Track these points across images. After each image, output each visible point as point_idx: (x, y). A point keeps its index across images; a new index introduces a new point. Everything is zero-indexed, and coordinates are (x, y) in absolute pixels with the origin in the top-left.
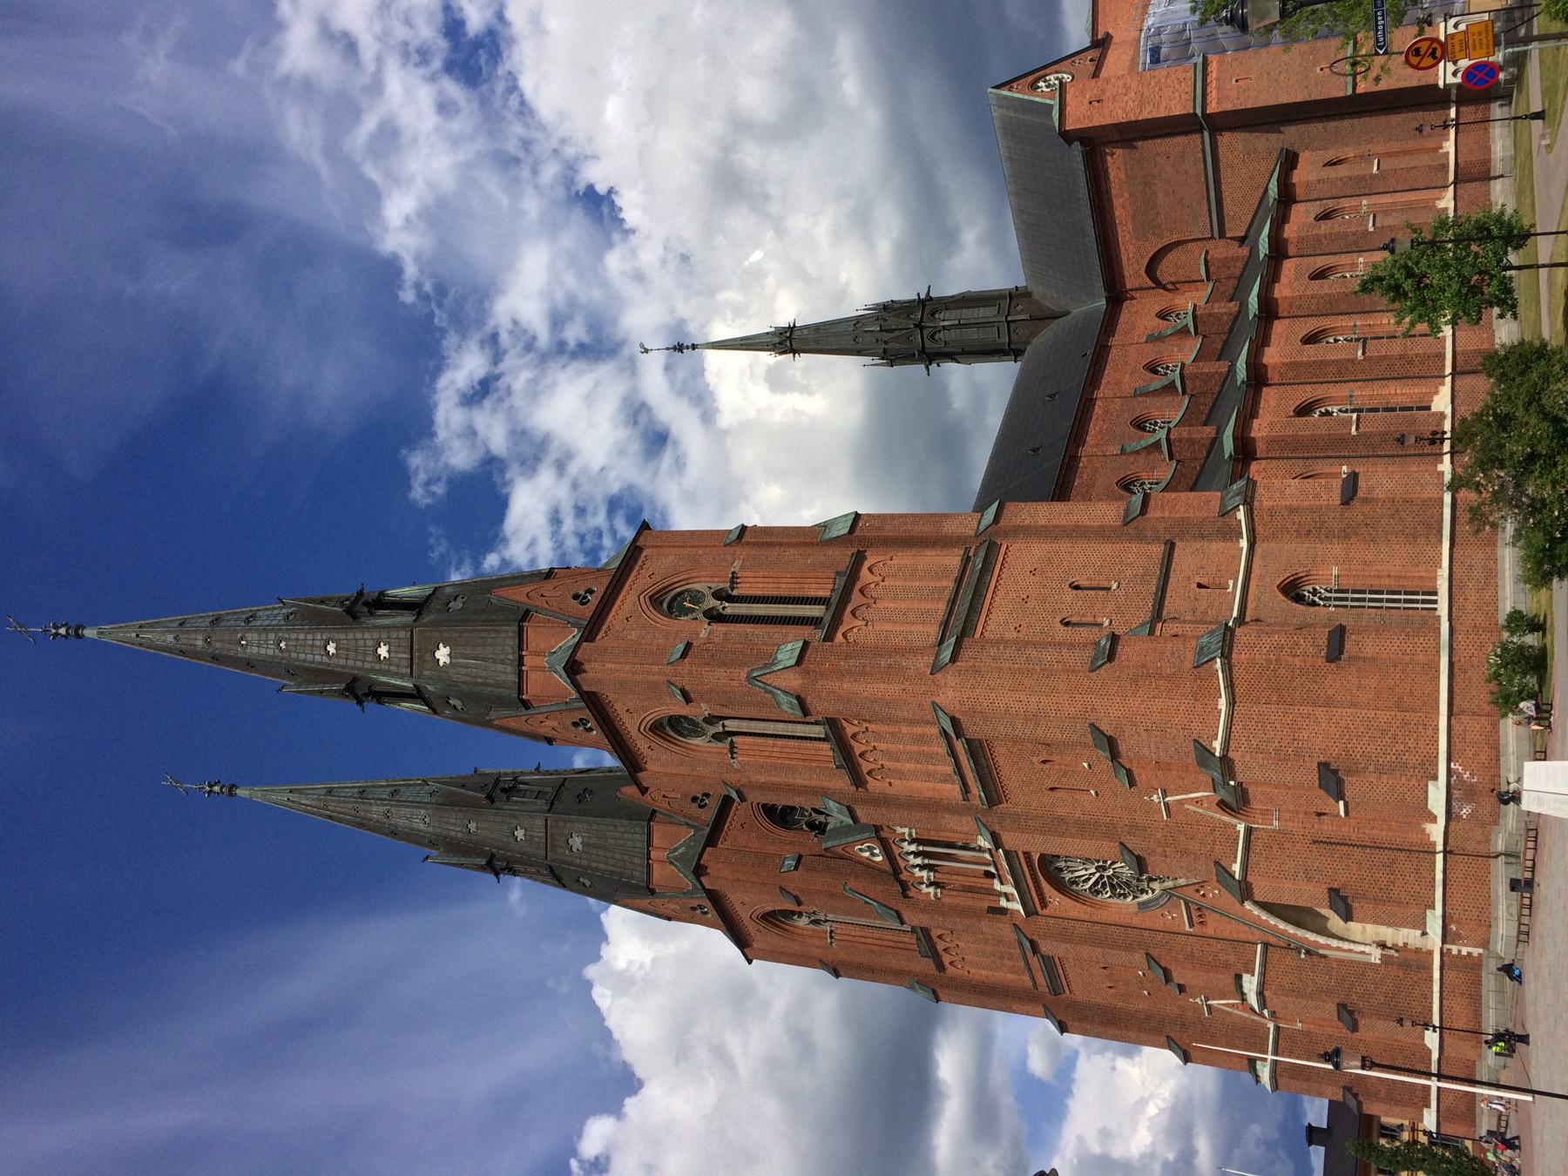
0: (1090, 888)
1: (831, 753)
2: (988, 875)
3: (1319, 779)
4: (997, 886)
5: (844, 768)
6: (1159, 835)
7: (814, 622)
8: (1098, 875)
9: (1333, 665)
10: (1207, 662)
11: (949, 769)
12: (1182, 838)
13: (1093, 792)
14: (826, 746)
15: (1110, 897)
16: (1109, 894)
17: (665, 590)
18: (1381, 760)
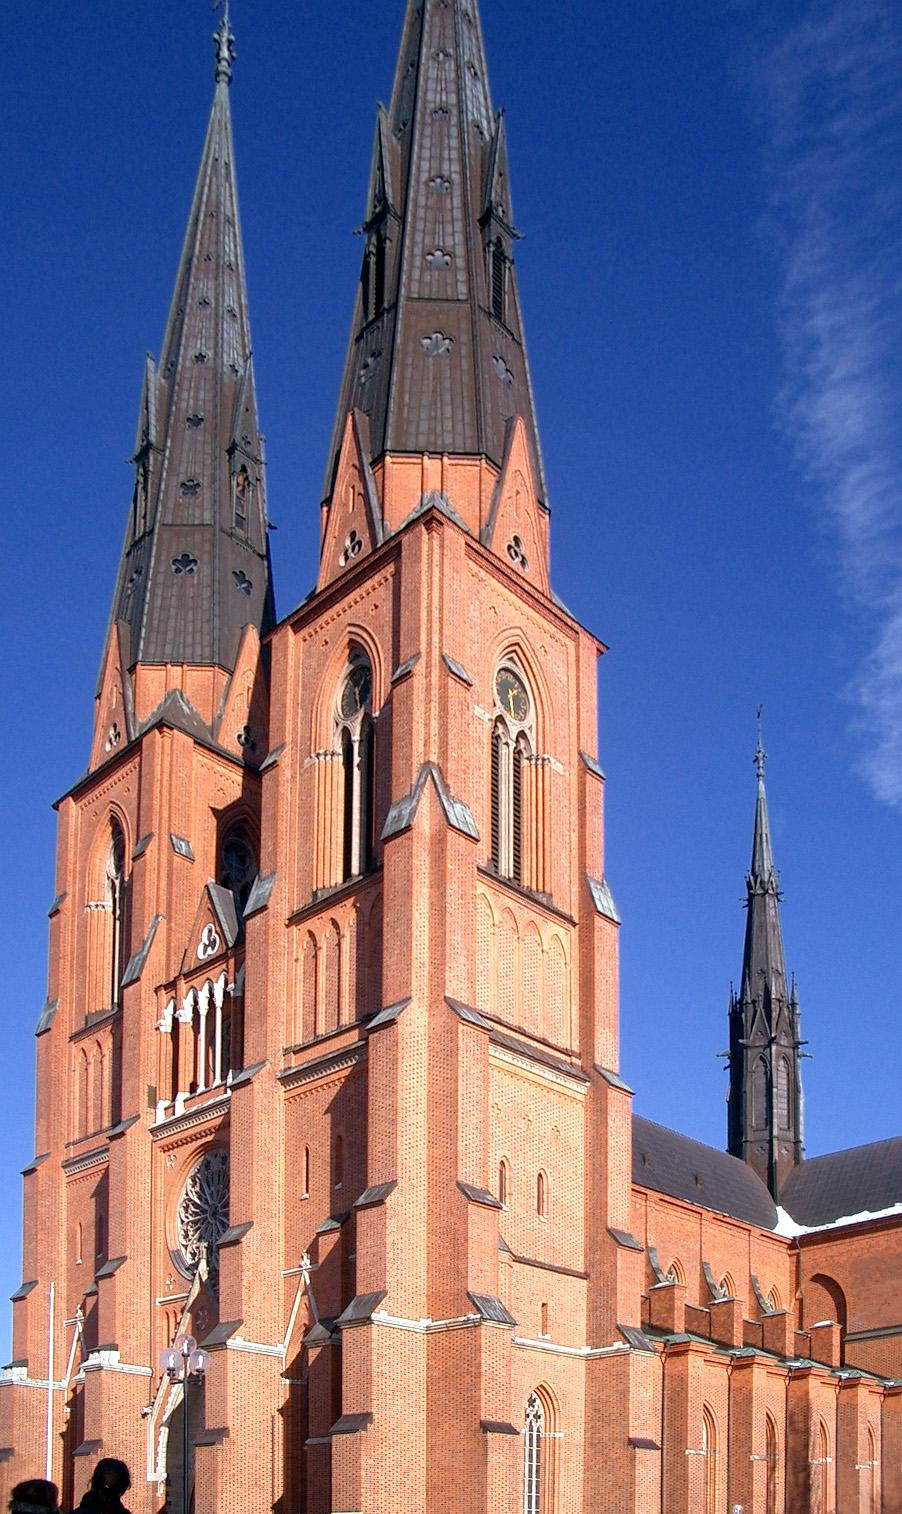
0: (190, 1200)
1: (333, 884)
2: (193, 1087)
3: (354, 1415)
4: (182, 1096)
5: (314, 901)
6: (263, 1265)
7: (495, 859)
8: (206, 1207)
9: (478, 1426)
10: (475, 1304)
11: (322, 1030)
12: (264, 1288)
13: (307, 1195)
14: (339, 878)
15: (182, 1222)
16: (186, 1220)
17: (528, 667)
18: (379, 1471)
